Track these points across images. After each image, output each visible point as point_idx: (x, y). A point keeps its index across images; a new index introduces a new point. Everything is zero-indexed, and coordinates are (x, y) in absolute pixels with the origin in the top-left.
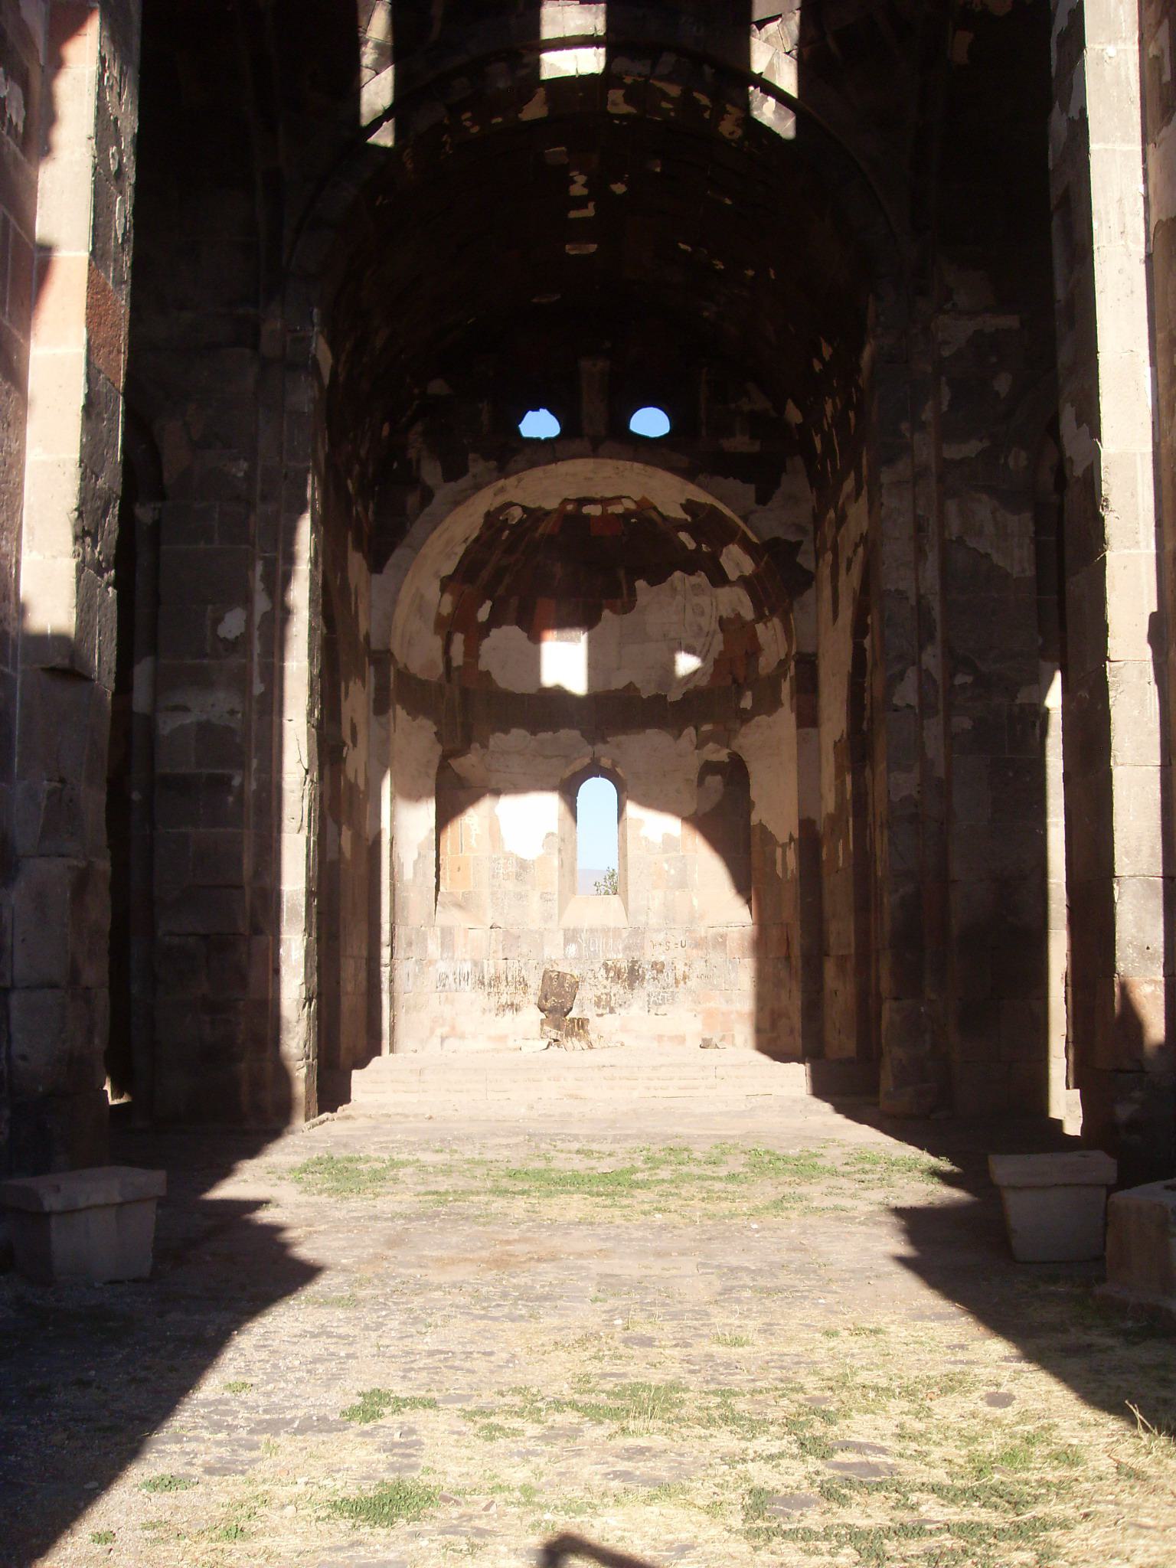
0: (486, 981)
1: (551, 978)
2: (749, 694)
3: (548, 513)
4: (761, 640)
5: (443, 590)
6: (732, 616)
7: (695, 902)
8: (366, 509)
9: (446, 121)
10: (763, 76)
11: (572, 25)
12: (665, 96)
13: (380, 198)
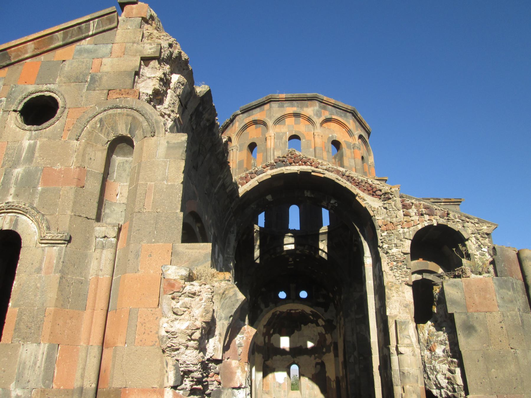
2: (325, 349)
3: (284, 312)
5: (264, 328)
7: (315, 392)
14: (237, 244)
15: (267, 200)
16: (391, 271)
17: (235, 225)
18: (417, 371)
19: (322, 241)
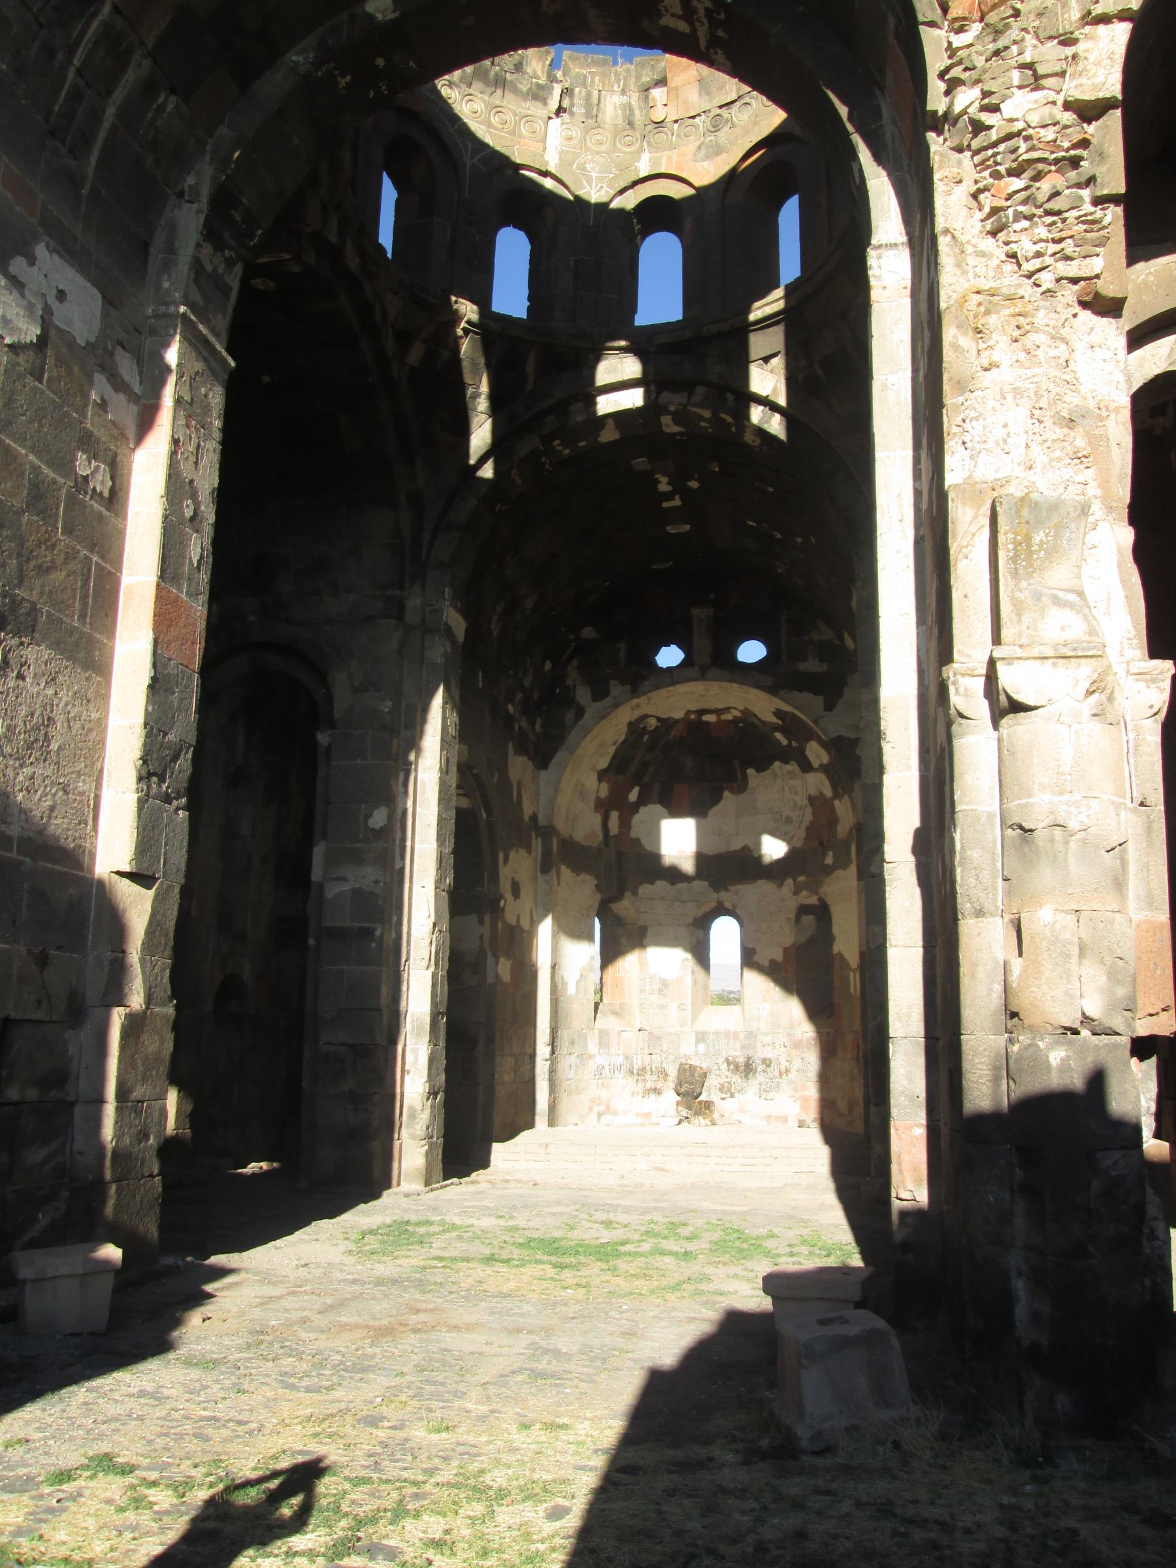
0: (635, 1071)
1: (685, 1070)
2: (831, 853)
3: (676, 721)
4: (838, 812)
5: (600, 780)
6: (817, 794)
8: (533, 724)
9: (541, 448)
10: (770, 398)
11: (629, 371)
12: (701, 418)
13: (499, 505)
14: (238, 269)
15: (371, 17)
16: (990, 239)
17: (208, 158)
18: (1124, 815)
19: (766, 360)
